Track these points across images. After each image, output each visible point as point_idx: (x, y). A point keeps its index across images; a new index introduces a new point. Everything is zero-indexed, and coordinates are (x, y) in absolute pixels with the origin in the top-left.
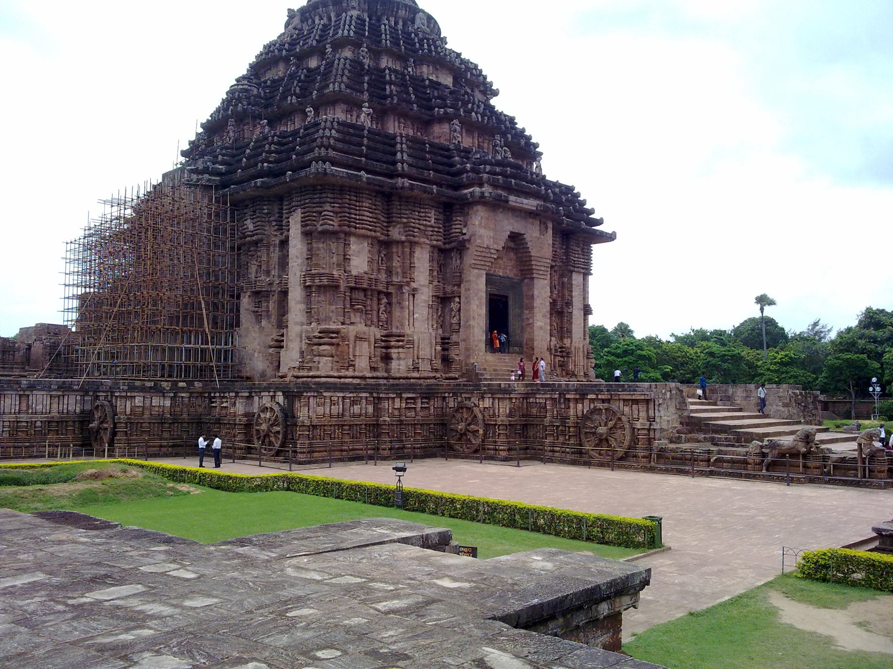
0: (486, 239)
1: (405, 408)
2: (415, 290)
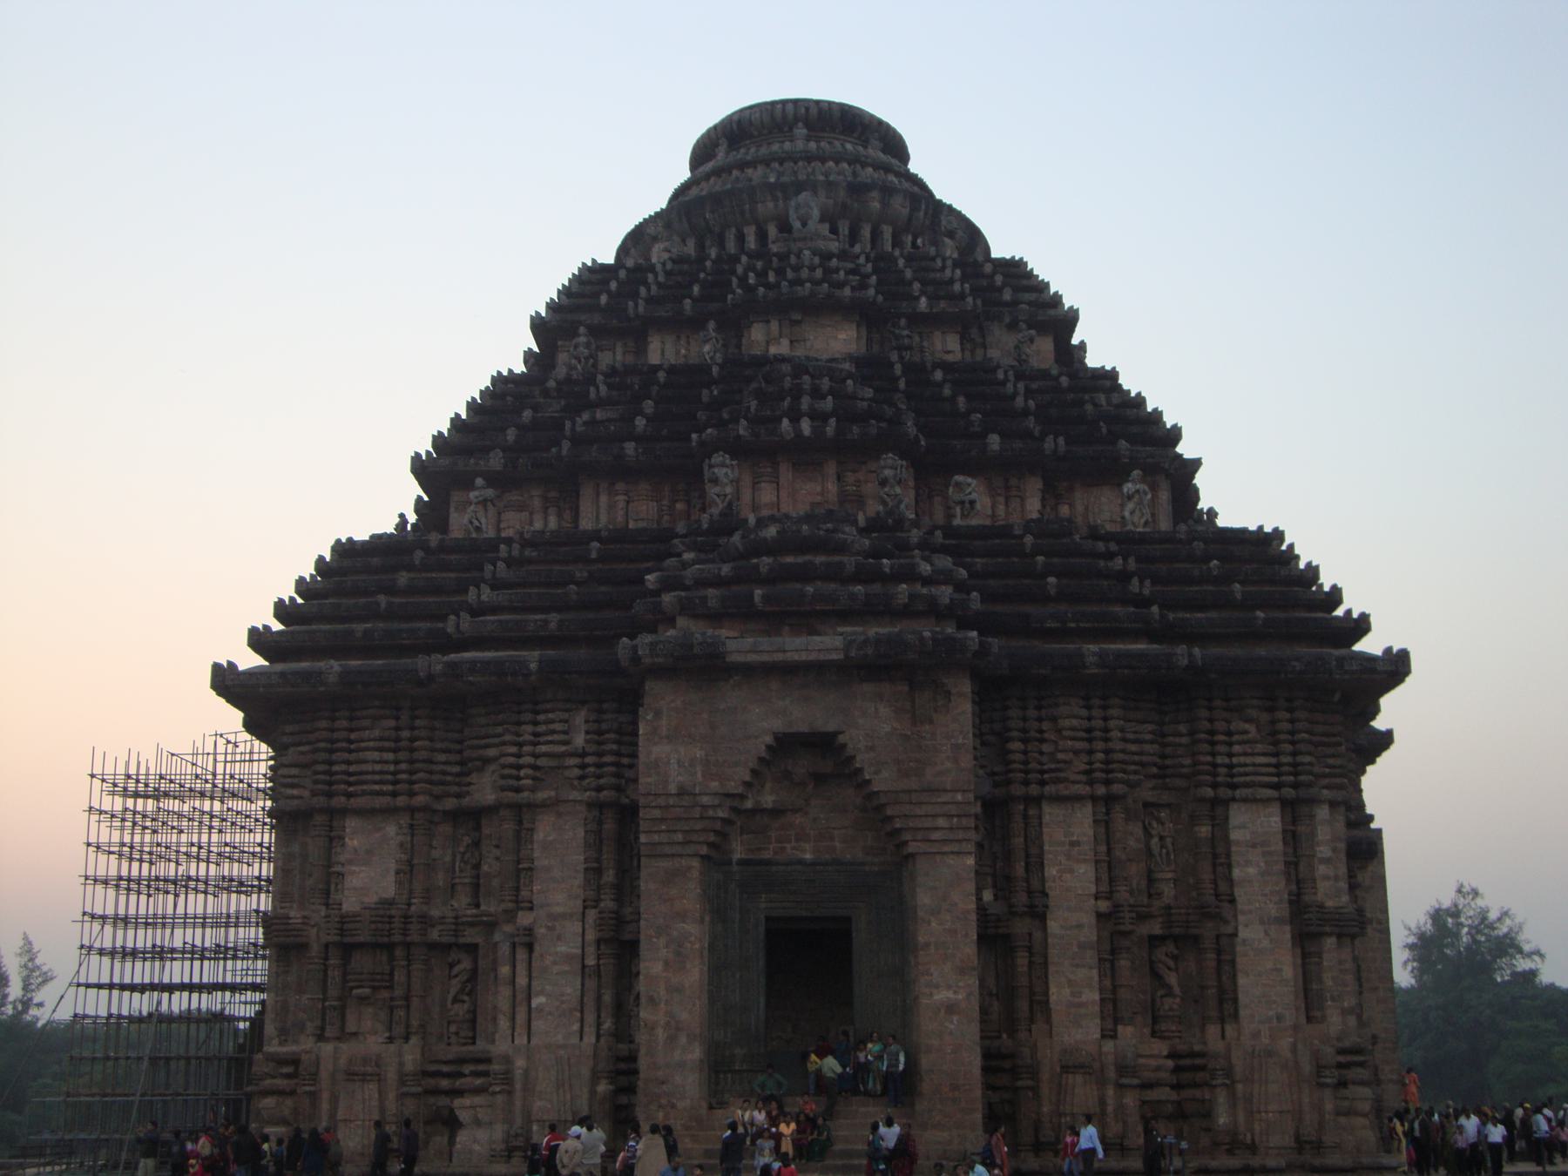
2: (529, 931)
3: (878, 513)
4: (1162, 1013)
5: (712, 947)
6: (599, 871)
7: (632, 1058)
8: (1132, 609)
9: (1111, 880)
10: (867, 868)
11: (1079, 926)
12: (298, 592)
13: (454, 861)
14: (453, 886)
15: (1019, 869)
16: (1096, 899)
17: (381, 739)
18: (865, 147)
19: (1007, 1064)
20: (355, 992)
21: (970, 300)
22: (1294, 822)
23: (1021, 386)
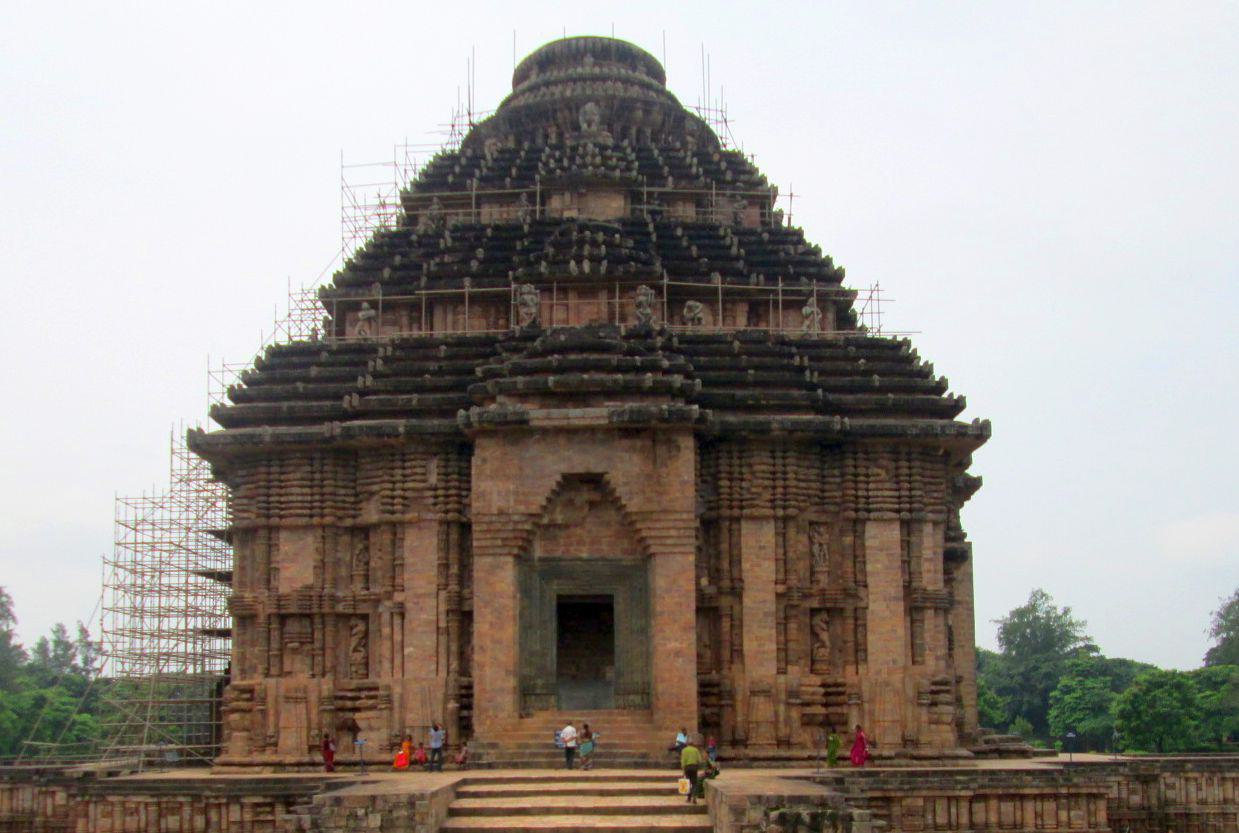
0: (495, 497)
1: (253, 822)
2: (401, 605)
3: (635, 326)
4: (818, 658)
5: (521, 615)
6: (447, 566)
7: (470, 687)
8: (804, 392)
9: (786, 571)
10: (624, 563)
11: (764, 601)
12: (246, 382)
13: (352, 562)
14: (352, 576)
15: (725, 565)
16: (776, 583)
17: (302, 479)
18: (634, 69)
19: (715, 690)
20: (290, 645)
21: (702, 179)
22: (909, 535)
23: (736, 240)
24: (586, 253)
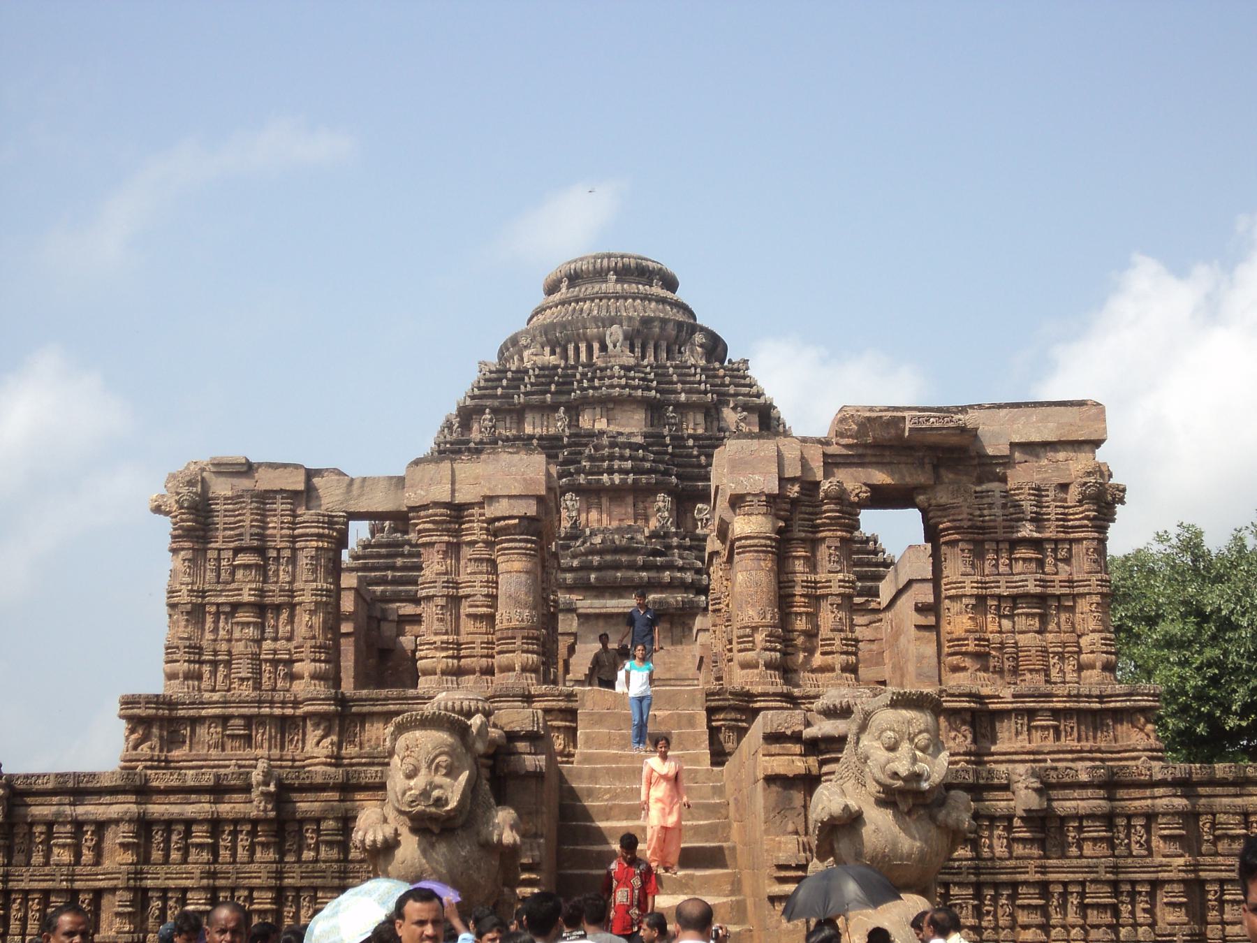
18: (651, 286)
24: (616, 467)
